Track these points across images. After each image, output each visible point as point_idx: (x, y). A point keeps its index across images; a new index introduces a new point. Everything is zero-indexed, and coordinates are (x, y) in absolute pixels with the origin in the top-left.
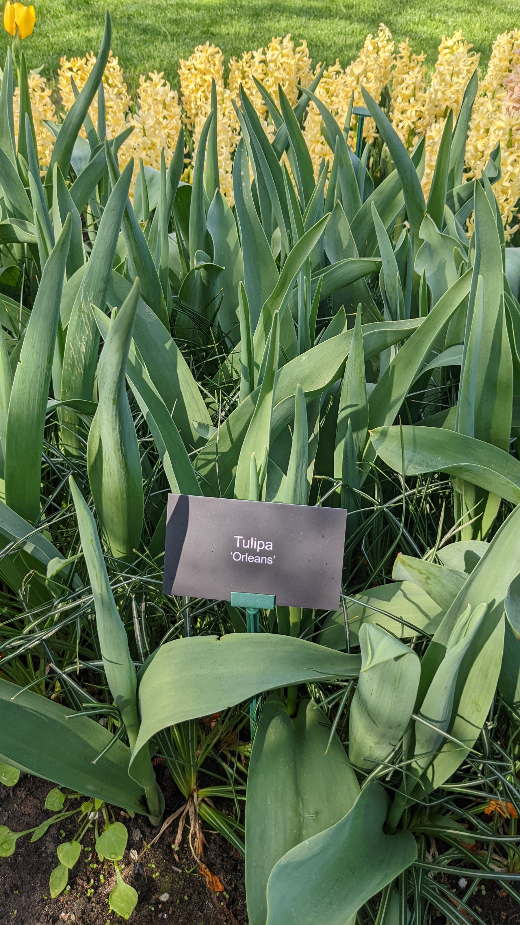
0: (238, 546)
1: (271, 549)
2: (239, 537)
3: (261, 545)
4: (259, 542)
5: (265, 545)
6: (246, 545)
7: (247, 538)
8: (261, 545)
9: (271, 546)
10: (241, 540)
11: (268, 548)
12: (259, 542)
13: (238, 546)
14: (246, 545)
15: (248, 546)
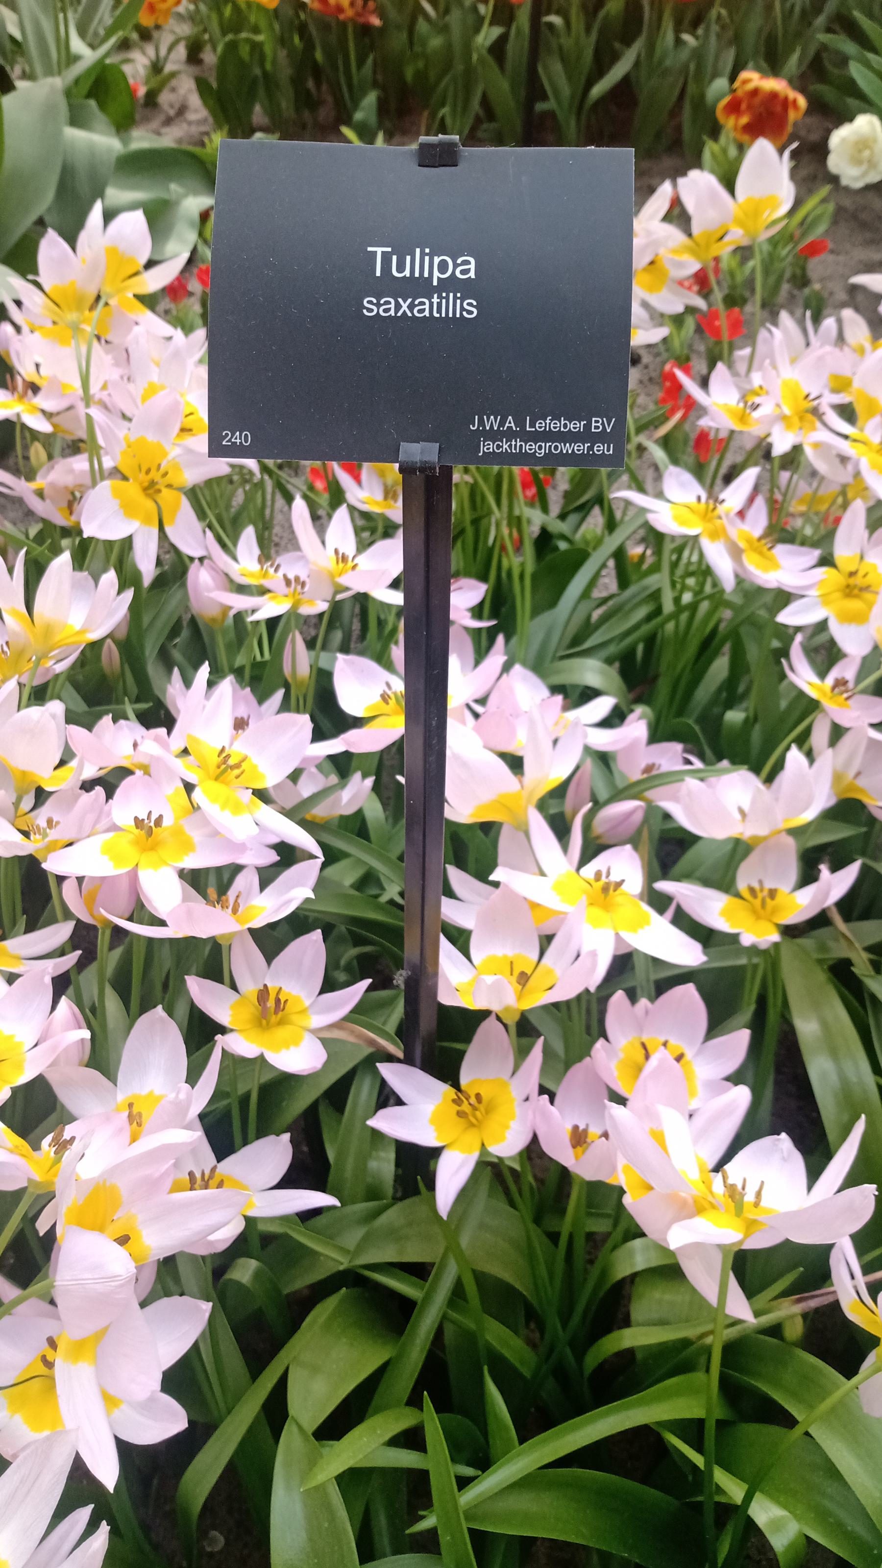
0: (378, 274)
1: (472, 274)
2: (379, 250)
3: (443, 267)
4: (437, 260)
5: (456, 266)
6: (401, 268)
7: (403, 250)
8: (443, 267)
9: (472, 266)
10: (386, 257)
11: (463, 272)
12: (437, 260)
13: (378, 274)
14: (401, 268)
15: (407, 273)
